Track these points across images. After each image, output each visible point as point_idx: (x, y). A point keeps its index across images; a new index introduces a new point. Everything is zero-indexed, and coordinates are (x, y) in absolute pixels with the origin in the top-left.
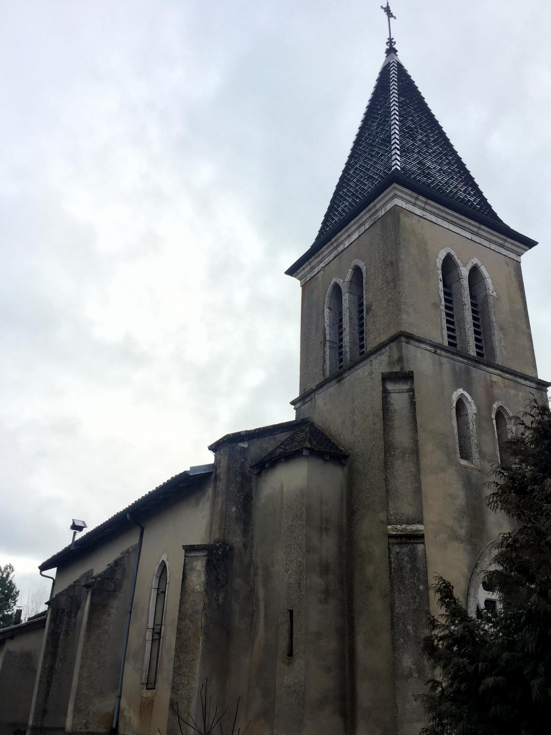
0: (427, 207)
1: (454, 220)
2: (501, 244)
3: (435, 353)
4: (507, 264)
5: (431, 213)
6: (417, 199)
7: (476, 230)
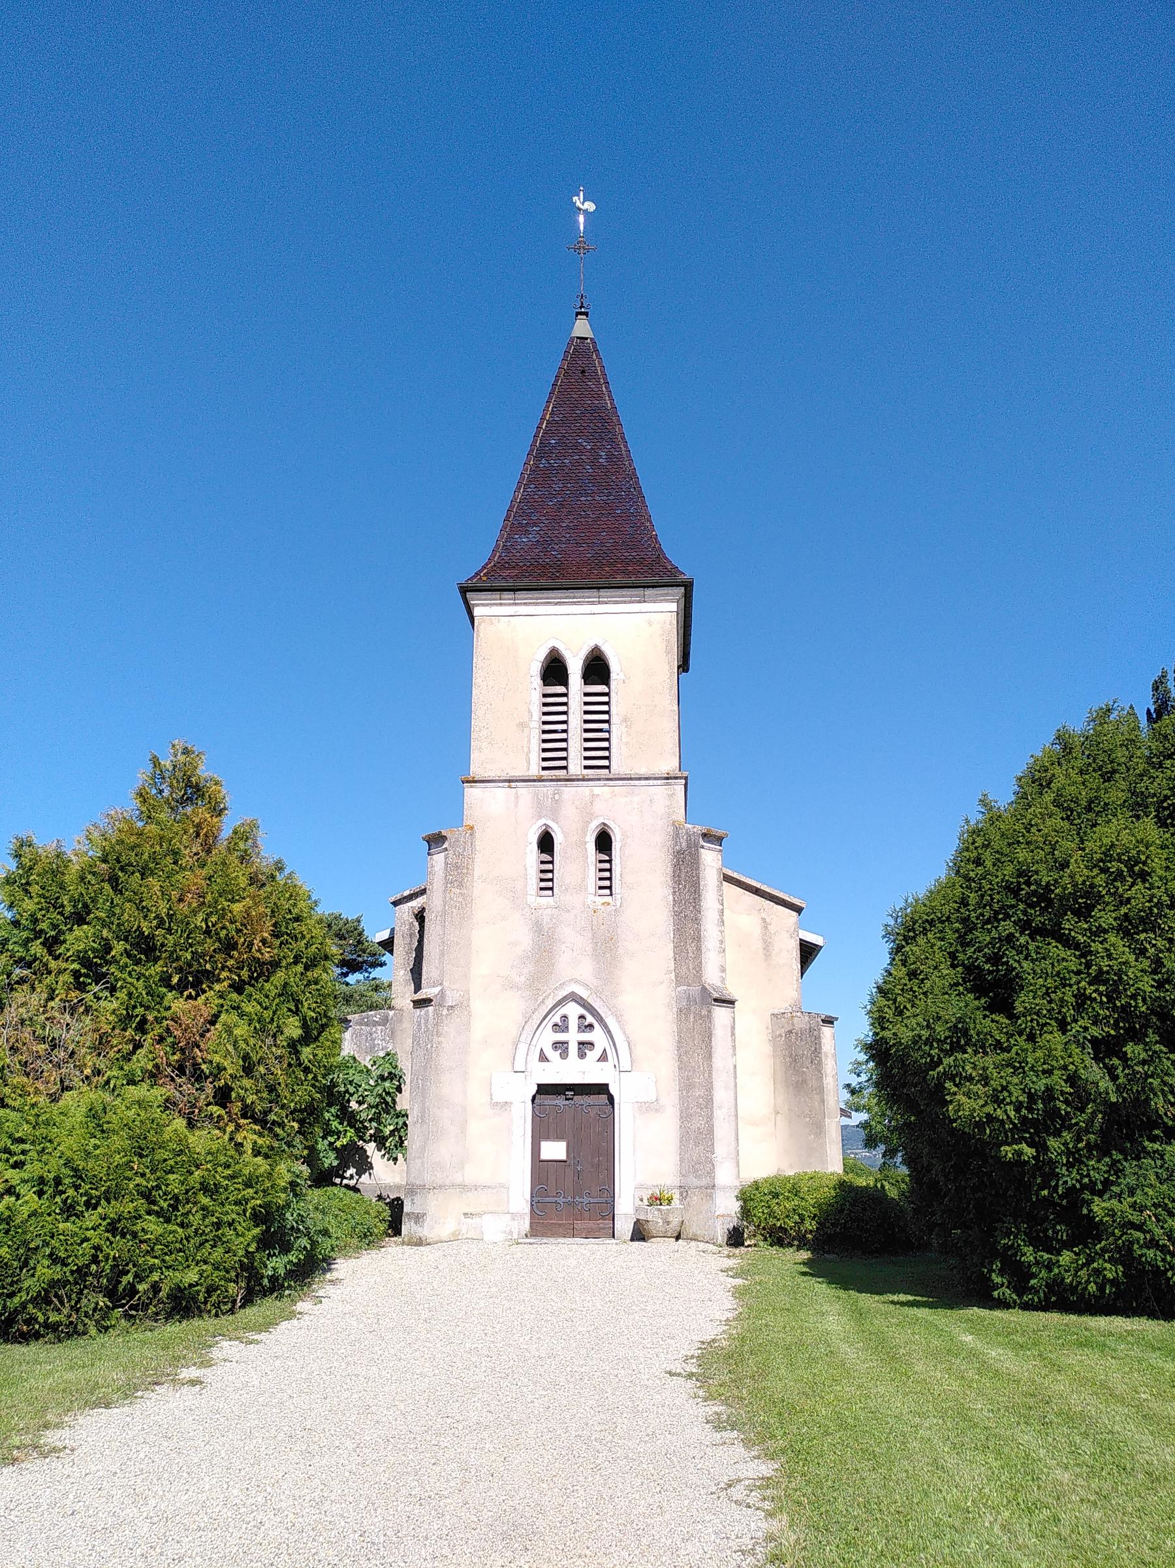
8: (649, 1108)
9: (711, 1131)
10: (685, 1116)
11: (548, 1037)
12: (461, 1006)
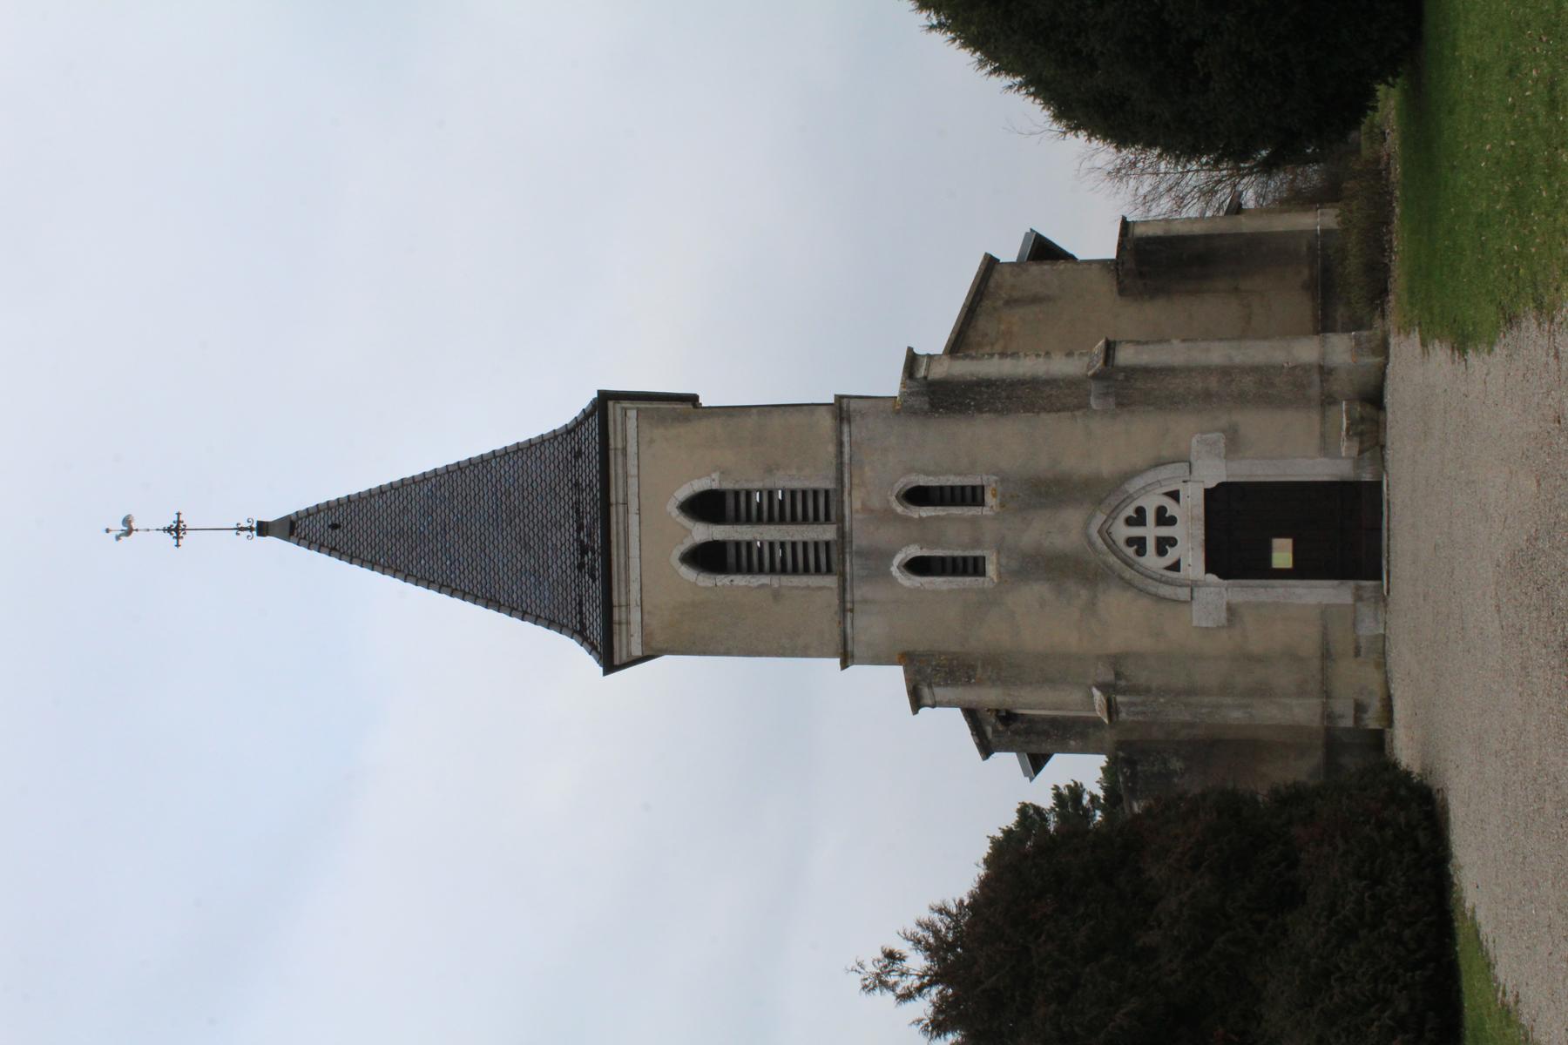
3: (852, 610)
4: (652, 441)
5: (628, 592)
7: (621, 508)
8: (1234, 444)
9: (1254, 369)
10: (1242, 400)
11: (1151, 560)
12: (1116, 662)
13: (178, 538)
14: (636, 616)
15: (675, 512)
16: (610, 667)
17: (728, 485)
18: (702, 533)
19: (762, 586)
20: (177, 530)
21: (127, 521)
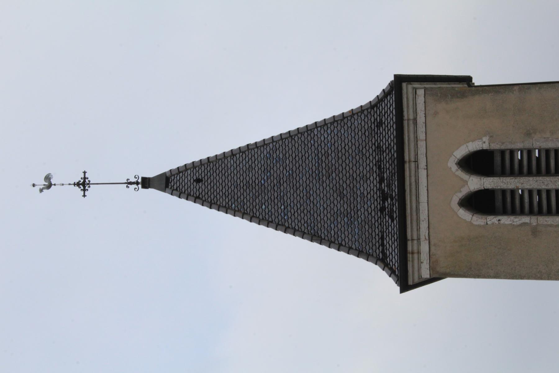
0: (415, 237)
1: (414, 198)
2: (414, 123)
4: (436, 113)
5: (418, 230)
6: (413, 253)
7: (413, 165)
13: (84, 190)
14: (424, 247)
15: (454, 168)
16: (405, 287)
17: (495, 146)
18: (475, 183)
19: (524, 224)
20: (84, 184)
21: (48, 178)
